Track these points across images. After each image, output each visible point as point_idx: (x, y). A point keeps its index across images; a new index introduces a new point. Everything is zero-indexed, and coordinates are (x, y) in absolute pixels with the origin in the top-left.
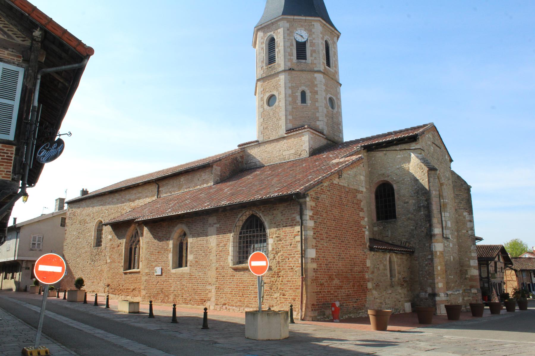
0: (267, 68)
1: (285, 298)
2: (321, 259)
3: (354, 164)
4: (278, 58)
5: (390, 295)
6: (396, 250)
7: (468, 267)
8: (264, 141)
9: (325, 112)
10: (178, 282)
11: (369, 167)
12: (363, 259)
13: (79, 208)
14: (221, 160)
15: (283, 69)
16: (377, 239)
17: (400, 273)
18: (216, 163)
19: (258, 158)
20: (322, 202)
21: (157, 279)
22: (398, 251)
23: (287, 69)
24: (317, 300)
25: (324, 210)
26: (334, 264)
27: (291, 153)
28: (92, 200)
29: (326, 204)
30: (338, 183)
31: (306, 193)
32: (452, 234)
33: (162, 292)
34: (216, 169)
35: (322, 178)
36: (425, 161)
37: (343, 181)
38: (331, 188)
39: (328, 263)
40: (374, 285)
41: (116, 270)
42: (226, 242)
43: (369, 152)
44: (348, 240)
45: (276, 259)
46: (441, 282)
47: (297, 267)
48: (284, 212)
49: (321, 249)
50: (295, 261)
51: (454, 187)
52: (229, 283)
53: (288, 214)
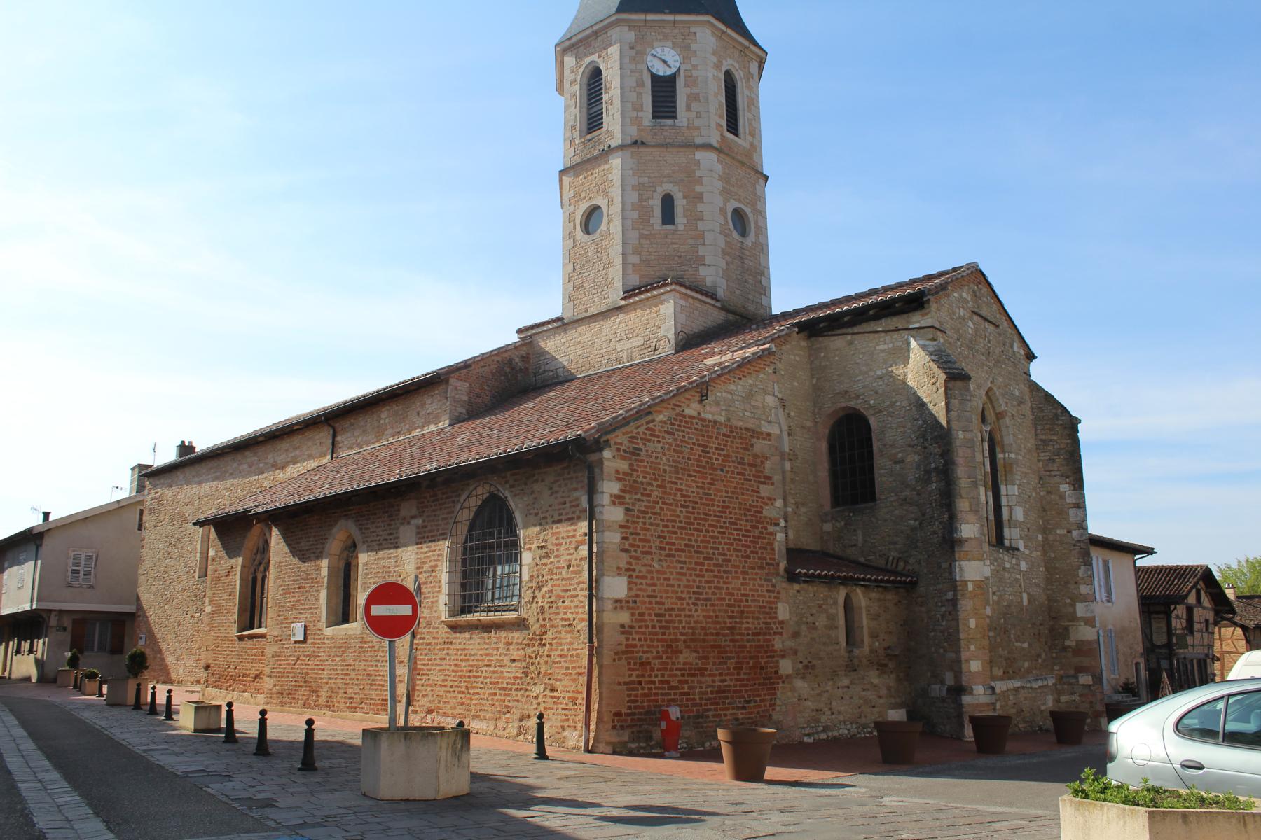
0: (584, 143)
1: (555, 697)
2: (644, 603)
3: (749, 366)
4: (607, 116)
5: (846, 689)
6: (864, 580)
7: (1070, 621)
8: (575, 318)
9: (723, 246)
10: (338, 659)
11: (812, 376)
12: (770, 602)
13: (171, 487)
14: (470, 366)
15: (619, 142)
16: (832, 552)
17: (877, 637)
18: (457, 374)
19: (560, 360)
20: (650, 460)
21: (296, 651)
22: (869, 580)
23: (629, 142)
24: (628, 702)
25: (656, 480)
26: (683, 613)
27: (634, 344)
28: (197, 467)
29: (661, 467)
30: (699, 414)
31: (602, 440)
32: (1027, 539)
33: (305, 682)
34: (456, 388)
35: (651, 402)
36: (941, 358)
37: (714, 409)
38: (676, 427)
39: (663, 612)
40: (800, 666)
41: (222, 630)
42: (435, 561)
43: (813, 339)
44: (724, 555)
45: (537, 603)
46: (977, 658)
47: (582, 620)
48: (556, 488)
49: (644, 577)
50: (576, 607)
51: (1036, 422)
52: (441, 659)
53: (563, 492)
